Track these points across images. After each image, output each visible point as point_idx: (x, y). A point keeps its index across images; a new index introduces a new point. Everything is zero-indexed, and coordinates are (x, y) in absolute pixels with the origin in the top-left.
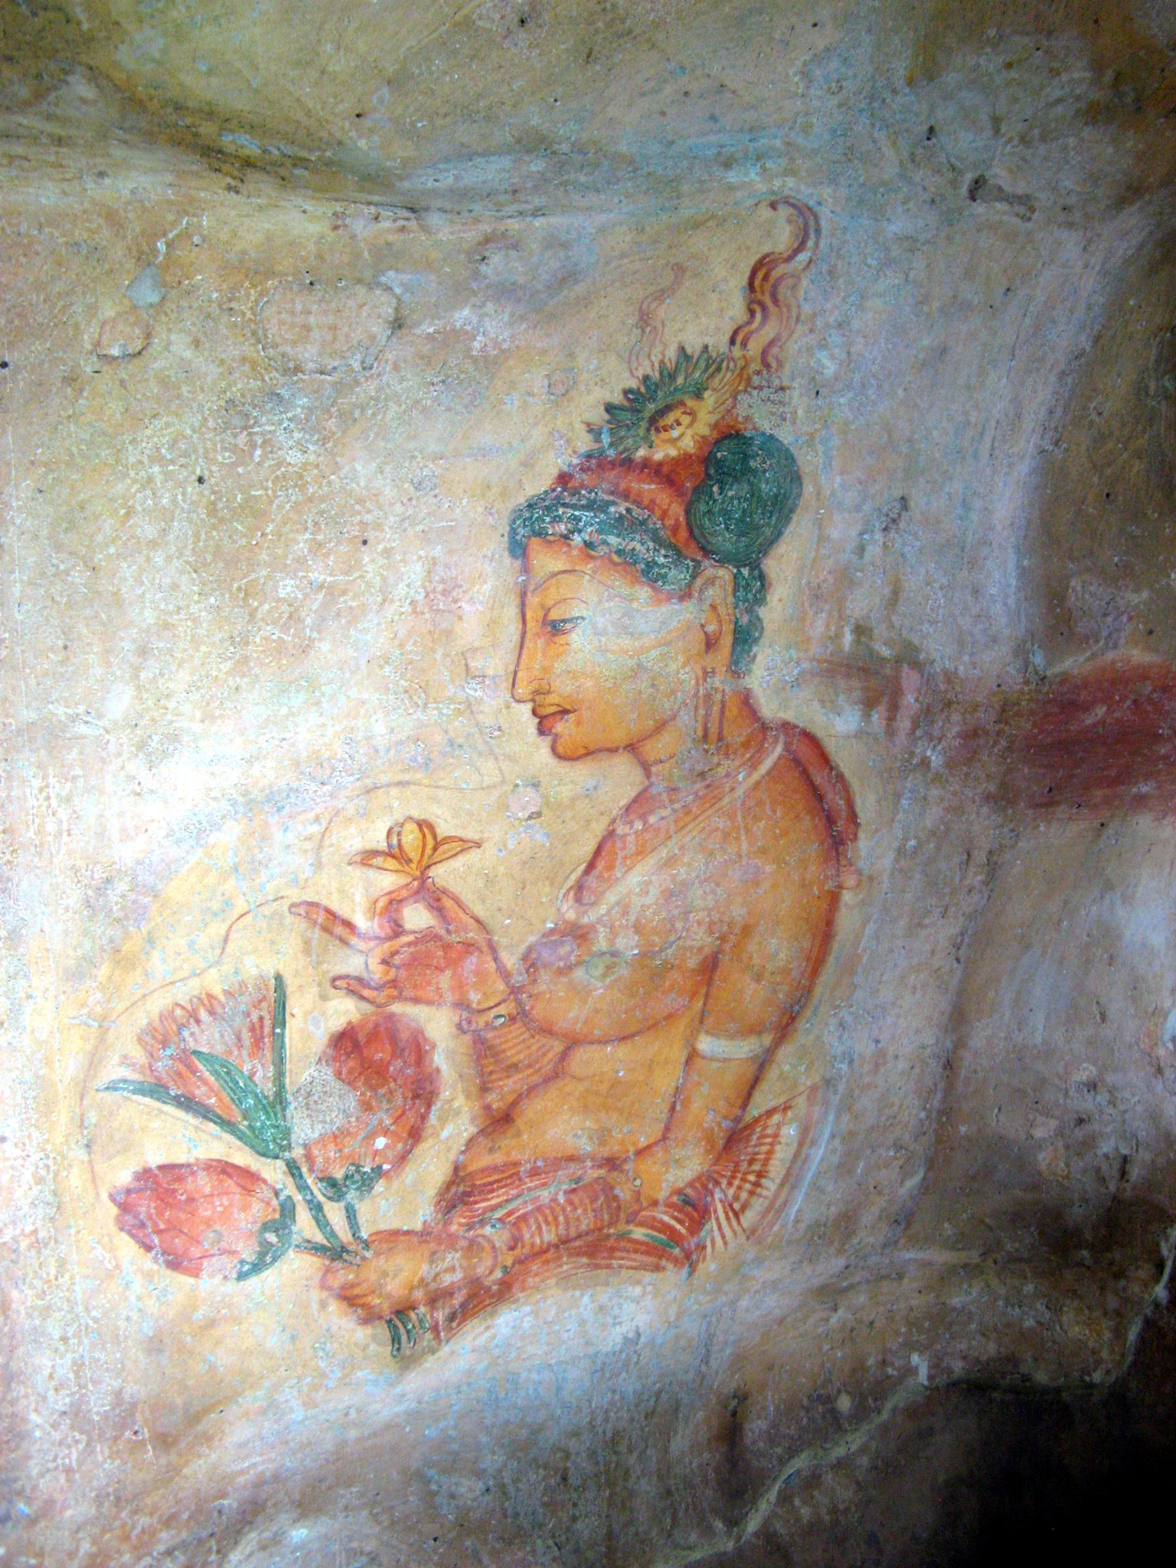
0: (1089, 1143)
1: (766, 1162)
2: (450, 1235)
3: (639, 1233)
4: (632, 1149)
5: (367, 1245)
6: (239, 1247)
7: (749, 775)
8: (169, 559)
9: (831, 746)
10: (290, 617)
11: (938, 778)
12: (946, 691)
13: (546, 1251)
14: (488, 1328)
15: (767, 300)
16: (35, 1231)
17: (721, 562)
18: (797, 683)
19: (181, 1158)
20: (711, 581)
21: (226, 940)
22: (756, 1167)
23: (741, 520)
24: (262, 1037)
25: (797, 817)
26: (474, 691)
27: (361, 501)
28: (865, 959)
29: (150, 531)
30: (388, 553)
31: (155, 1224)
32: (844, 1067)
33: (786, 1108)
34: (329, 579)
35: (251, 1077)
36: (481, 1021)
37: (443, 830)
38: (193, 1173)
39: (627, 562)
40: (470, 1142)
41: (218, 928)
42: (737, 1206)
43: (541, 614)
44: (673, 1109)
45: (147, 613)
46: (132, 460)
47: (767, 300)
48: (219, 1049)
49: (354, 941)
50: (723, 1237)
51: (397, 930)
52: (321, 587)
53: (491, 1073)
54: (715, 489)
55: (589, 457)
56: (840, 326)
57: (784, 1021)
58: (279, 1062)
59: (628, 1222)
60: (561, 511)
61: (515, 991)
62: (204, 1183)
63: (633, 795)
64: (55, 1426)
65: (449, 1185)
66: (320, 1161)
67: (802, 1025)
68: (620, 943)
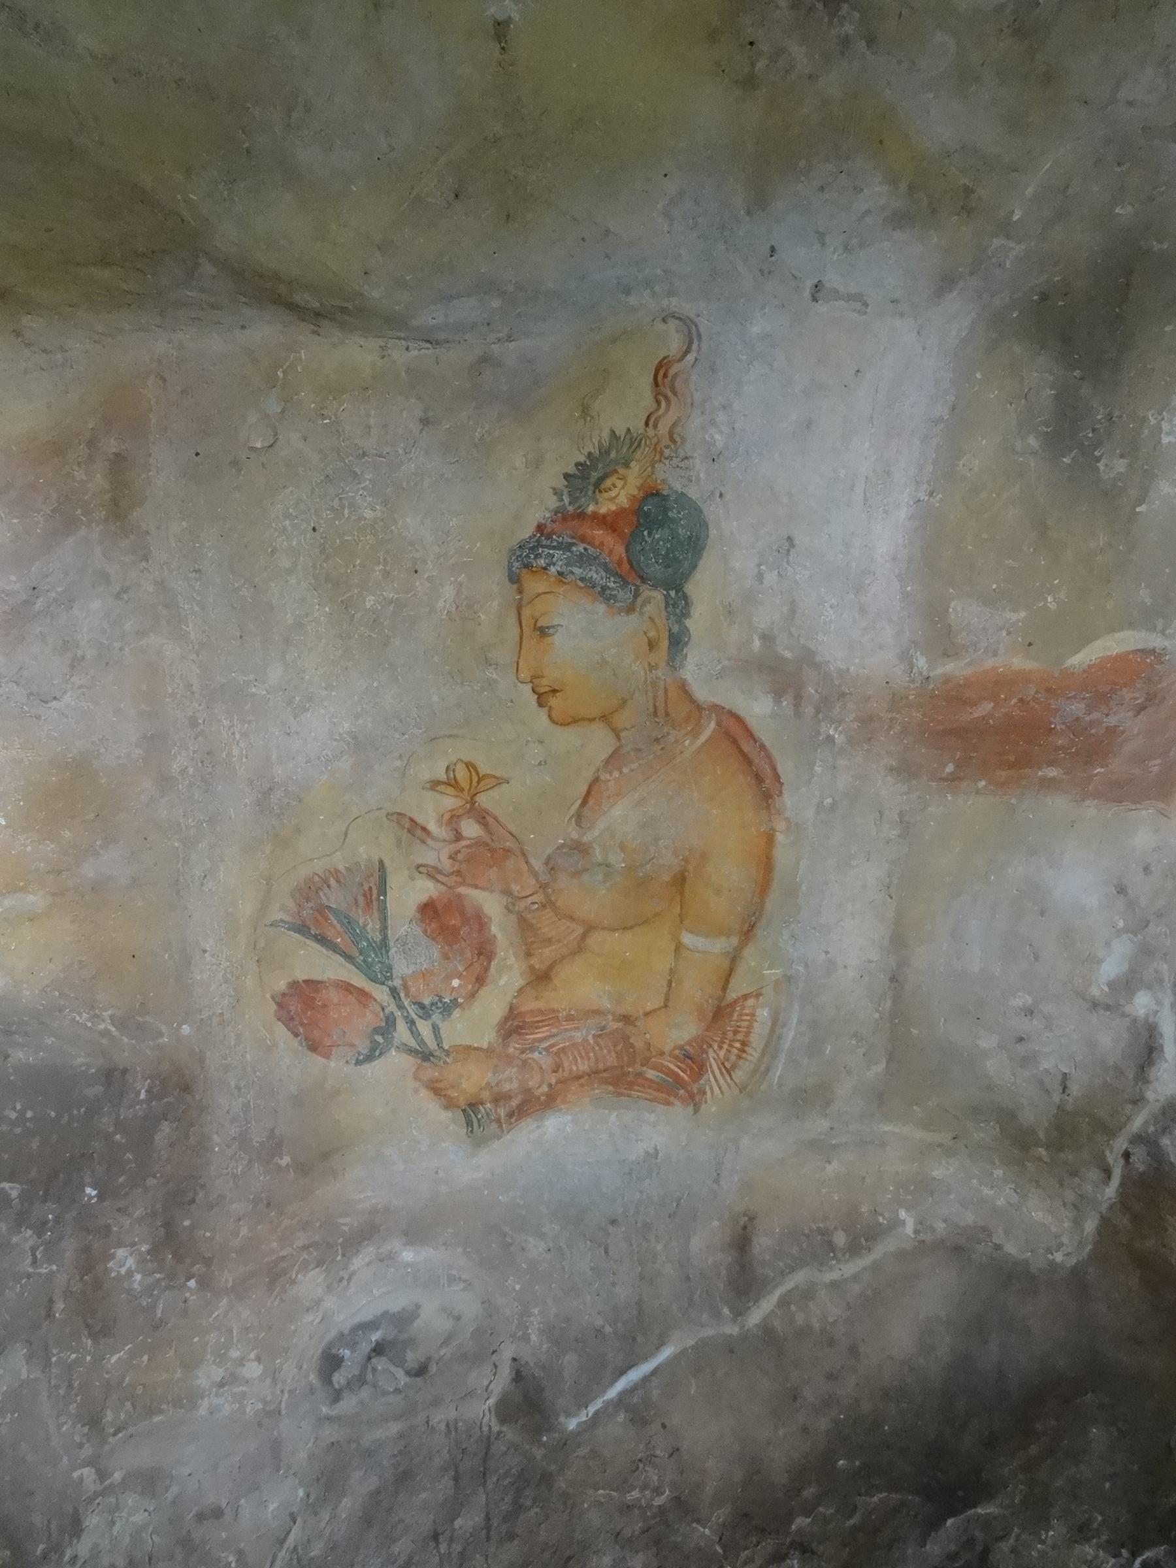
0: (1028, 1060)
1: (748, 1033)
2: (508, 1056)
3: (651, 1074)
7: (692, 743)
8: (299, 583)
12: (840, 685)
13: (580, 1077)
14: (538, 1127)
16: (222, 1014)
17: (655, 587)
19: (316, 976)
20: (648, 600)
21: (346, 834)
22: (740, 1037)
23: (666, 556)
26: (491, 674)
28: (804, 888)
29: (286, 563)
35: (365, 926)
36: (521, 905)
37: (484, 769)
39: (589, 585)
40: (521, 991)
42: (728, 1065)
44: (670, 985)
49: (429, 841)
50: (718, 1085)
51: (458, 837)
52: (392, 601)
53: (533, 943)
54: (645, 533)
55: (556, 513)
57: (745, 929)
58: (384, 919)
59: (642, 1065)
60: (540, 550)
61: (543, 886)
62: (334, 995)
64: (228, 1146)
65: (506, 1019)
68: (612, 858)
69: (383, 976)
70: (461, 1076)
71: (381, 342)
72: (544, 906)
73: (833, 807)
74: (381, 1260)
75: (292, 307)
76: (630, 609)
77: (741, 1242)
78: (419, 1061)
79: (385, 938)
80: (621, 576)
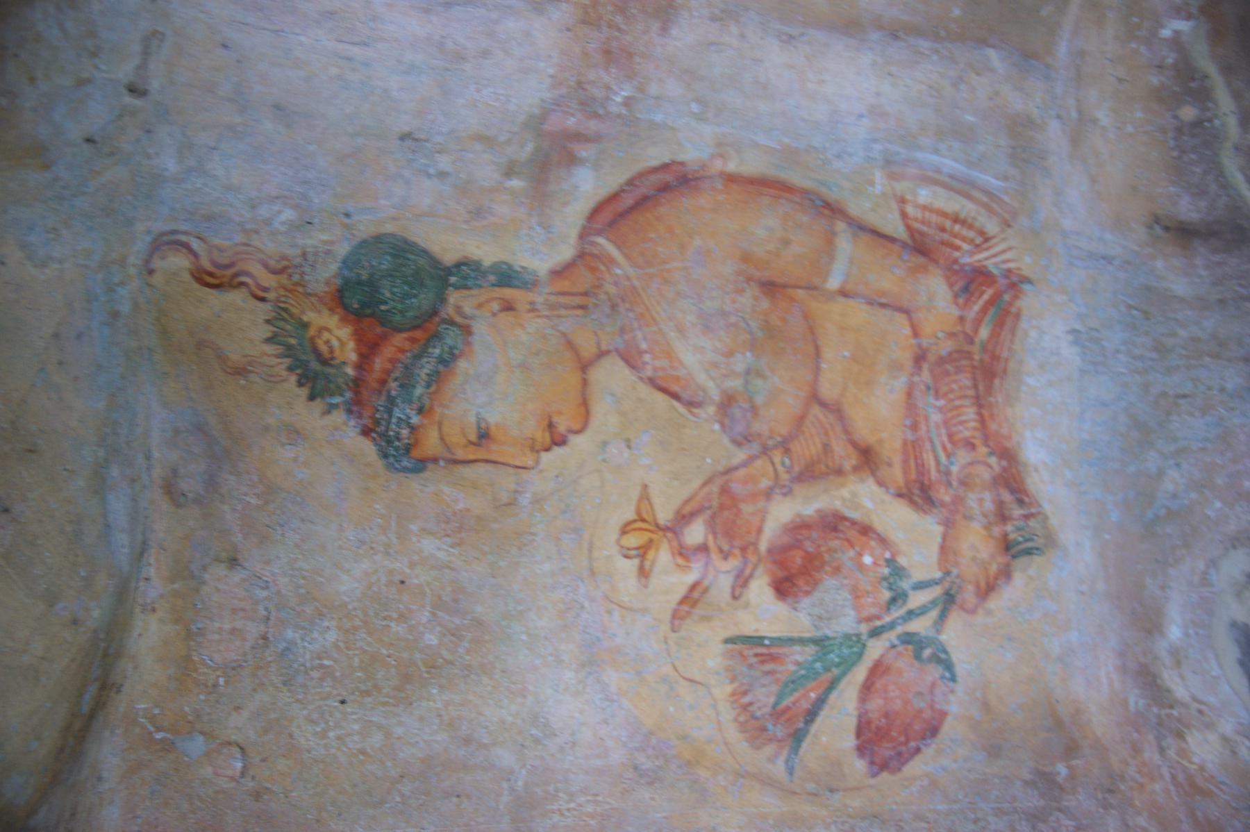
3: (984, 333)
4: (913, 341)
5: (947, 573)
6: (929, 679)
7: (618, 265)
8: (400, 723)
9: (603, 193)
10: (453, 635)
11: (641, 89)
14: (1037, 470)
15: (229, 272)
17: (443, 300)
18: (547, 228)
19: (852, 722)
20: (458, 309)
22: (948, 224)
24: (770, 655)
25: (657, 219)
26: (525, 500)
27: (370, 586)
28: (786, 140)
30: (412, 565)
31: (902, 744)
32: (877, 147)
33: (903, 201)
34: (428, 608)
35: (798, 663)
36: (784, 477)
37: (631, 515)
38: (866, 712)
39: (436, 379)
40: (881, 483)
41: (683, 688)
43: (472, 448)
44: (883, 305)
45: (439, 738)
46: (323, 751)
47: (229, 272)
48: (774, 688)
49: (706, 583)
50: (1003, 252)
51: (703, 548)
52: (434, 614)
54: (383, 308)
55: (350, 412)
56: (253, 207)
57: (827, 212)
58: (791, 641)
63: (621, 363)
65: (912, 503)
66: (874, 611)
67: (833, 195)
69: (856, 644)
70: (974, 559)
71: (138, 610)
72: (787, 451)
73: (698, 100)
74: (1178, 664)
75: (92, 716)
76: (467, 330)
77: (1183, 234)
78: (955, 607)
79: (816, 641)
80: (428, 340)
